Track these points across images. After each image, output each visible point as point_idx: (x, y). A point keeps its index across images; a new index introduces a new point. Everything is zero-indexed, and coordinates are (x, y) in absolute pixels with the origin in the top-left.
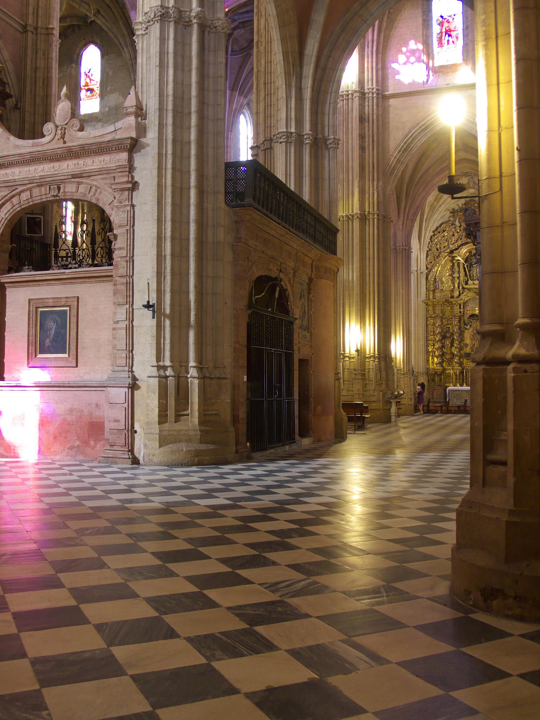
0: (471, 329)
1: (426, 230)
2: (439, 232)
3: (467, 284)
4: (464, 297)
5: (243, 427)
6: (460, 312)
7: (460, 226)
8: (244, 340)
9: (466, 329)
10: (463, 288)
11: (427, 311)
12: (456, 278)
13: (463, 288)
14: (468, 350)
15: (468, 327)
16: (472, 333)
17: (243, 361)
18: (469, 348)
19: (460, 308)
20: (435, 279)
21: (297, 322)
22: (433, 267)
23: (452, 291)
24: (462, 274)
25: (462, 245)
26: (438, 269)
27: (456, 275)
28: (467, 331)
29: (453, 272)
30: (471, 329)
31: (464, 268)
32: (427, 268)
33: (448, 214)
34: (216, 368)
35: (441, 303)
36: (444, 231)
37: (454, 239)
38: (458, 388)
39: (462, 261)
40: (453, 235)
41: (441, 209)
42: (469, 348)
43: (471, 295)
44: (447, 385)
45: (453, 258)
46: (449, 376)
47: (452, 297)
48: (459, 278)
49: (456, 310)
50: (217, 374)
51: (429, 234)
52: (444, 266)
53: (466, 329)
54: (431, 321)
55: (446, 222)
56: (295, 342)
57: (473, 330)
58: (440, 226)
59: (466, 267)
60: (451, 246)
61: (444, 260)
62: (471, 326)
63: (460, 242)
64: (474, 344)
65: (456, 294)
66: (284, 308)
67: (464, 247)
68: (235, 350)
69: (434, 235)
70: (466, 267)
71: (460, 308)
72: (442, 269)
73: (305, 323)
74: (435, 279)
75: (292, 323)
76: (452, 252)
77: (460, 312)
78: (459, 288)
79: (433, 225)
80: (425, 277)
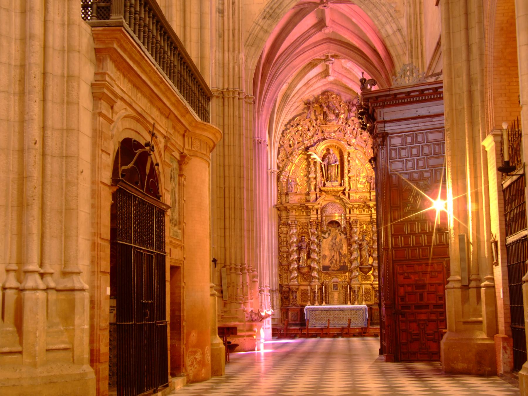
0: (330, 238)
1: (277, 123)
2: (292, 126)
3: (324, 185)
4: (323, 201)
5: (105, 368)
6: (317, 218)
7: (316, 120)
8: (106, 233)
9: (324, 238)
10: (321, 191)
11: (280, 217)
12: (312, 180)
13: (321, 191)
14: (327, 263)
15: (327, 235)
16: (331, 243)
17: (106, 265)
18: (327, 260)
19: (317, 213)
20: (288, 180)
21: (169, 212)
22: (285, 166)
23: (308, 194)
24: (319, 175)
25: (319, 141)
26: (290, 168)
27: (312, 175)
28: (325, 240)
29: (309, 172)
30: (330, 238)
31: (321, 168)
32: (279, 167)
33: (303, 106)
34: (65, 274)
35: (296, 207)
36: (298, 125)
37: (309, 134)
38: (317, 306)
39: (319, 160)
40: (309, 130)
41: (294, 99)
42: (327, 260)
43: (330, 198)
44: (303, 304)
45: (309, 156)
46: (304, 293)
47: (308, 201)
48: (315, 178)
49: (313, 217)
50: (67, 283)
51: (281, 128)
52: (297, 166)
53: (324, 238)
54: (284, 229)
55: (300, 115)
56: (167, 240)
57: (332, 239)
58: (293, 119)
59: (323, 166)
60: (306, 142)
61: (298, 159)
62: (329, 234)
63: (316, 138)
64: (334, 256)
65: (313, 197)
66: (154, 190)
67: (322, 143)
68: (94, 246)
69: (287, 129)
70: (323, 166)
71: (317, 213)
72: (296, 169)
73: (176, 217)
74: (288, 180)
75: (162, 213)
76: (307, 149)
77: (317, 218)
78: (315, 190)
79: (286, 117)
80: (276, 177)
